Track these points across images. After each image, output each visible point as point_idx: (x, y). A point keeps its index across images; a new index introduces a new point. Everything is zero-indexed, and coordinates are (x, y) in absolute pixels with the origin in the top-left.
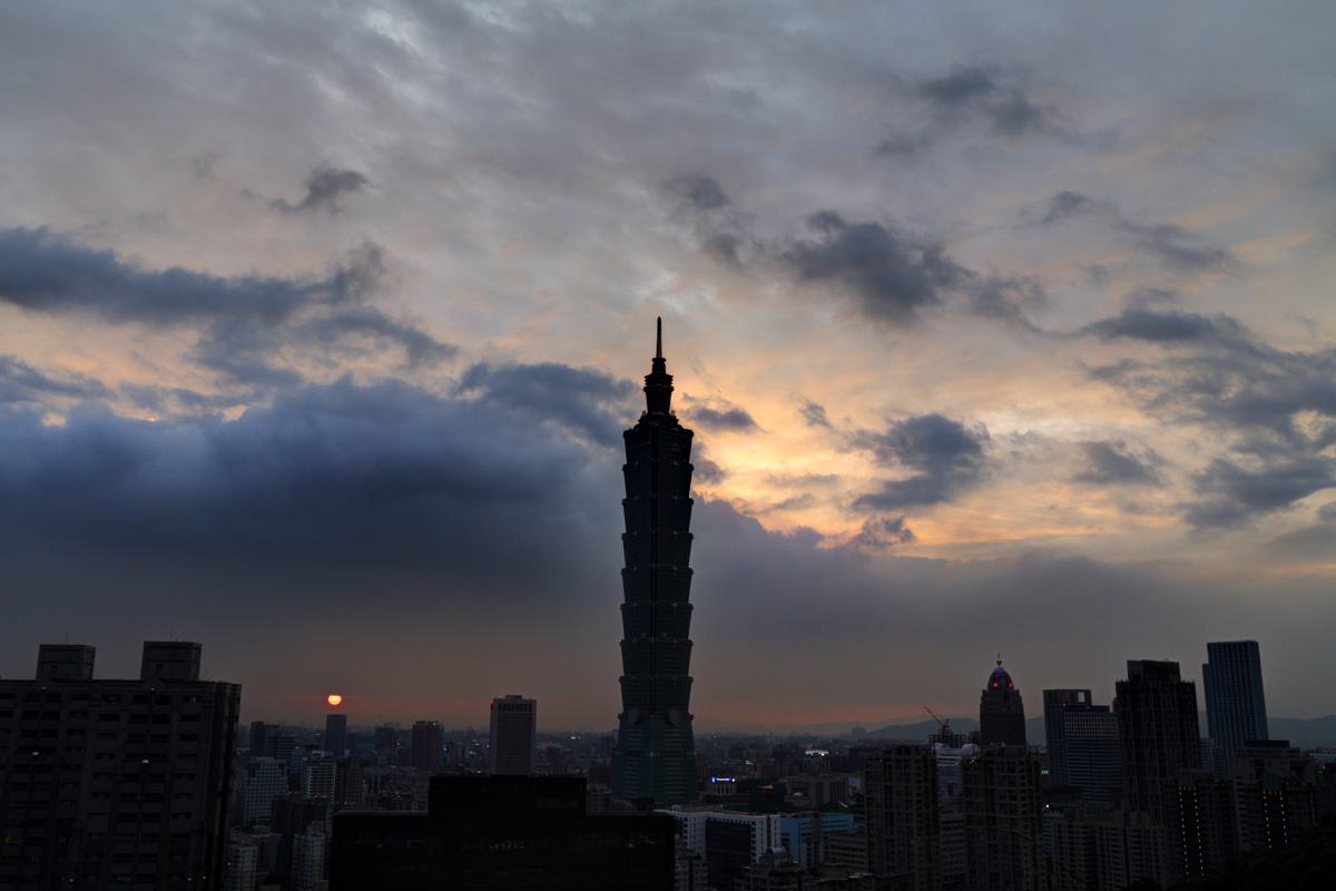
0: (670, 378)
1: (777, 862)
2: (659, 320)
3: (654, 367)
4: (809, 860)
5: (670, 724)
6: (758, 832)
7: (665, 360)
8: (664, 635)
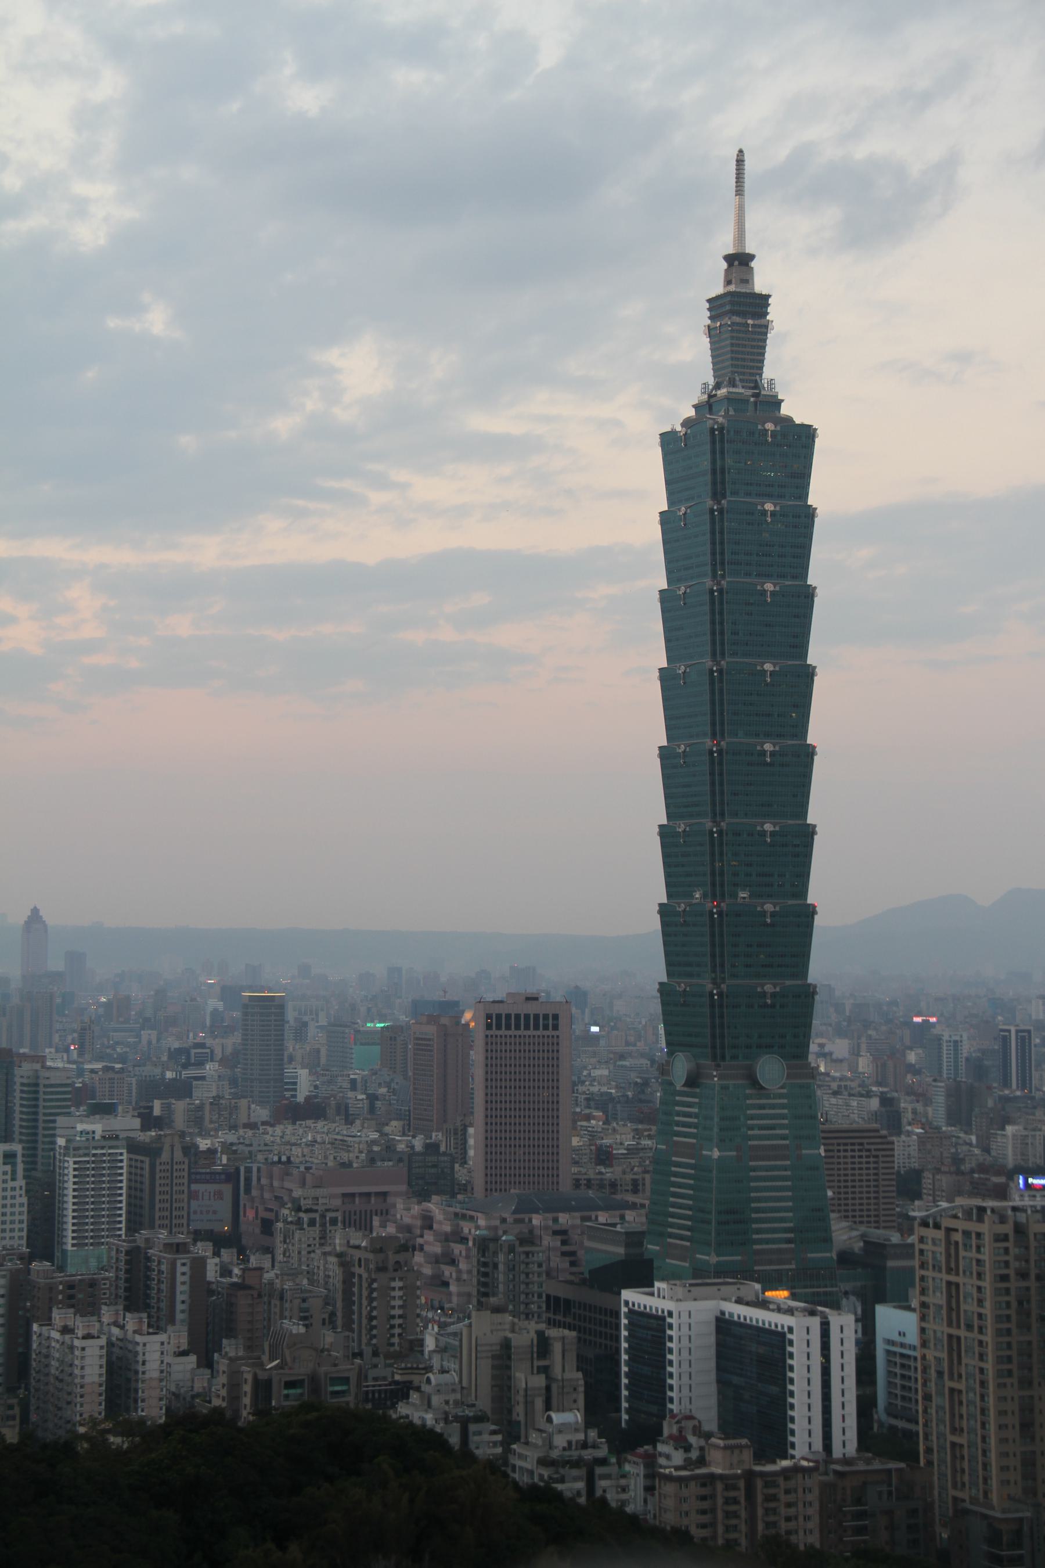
0: (763, 300)
1: (560, 1441)
2: (740, 162)
3: (728, 282)
5: (755, 1083)
6: (797, 1349)
7: (752, 257)
8: (742, 895)
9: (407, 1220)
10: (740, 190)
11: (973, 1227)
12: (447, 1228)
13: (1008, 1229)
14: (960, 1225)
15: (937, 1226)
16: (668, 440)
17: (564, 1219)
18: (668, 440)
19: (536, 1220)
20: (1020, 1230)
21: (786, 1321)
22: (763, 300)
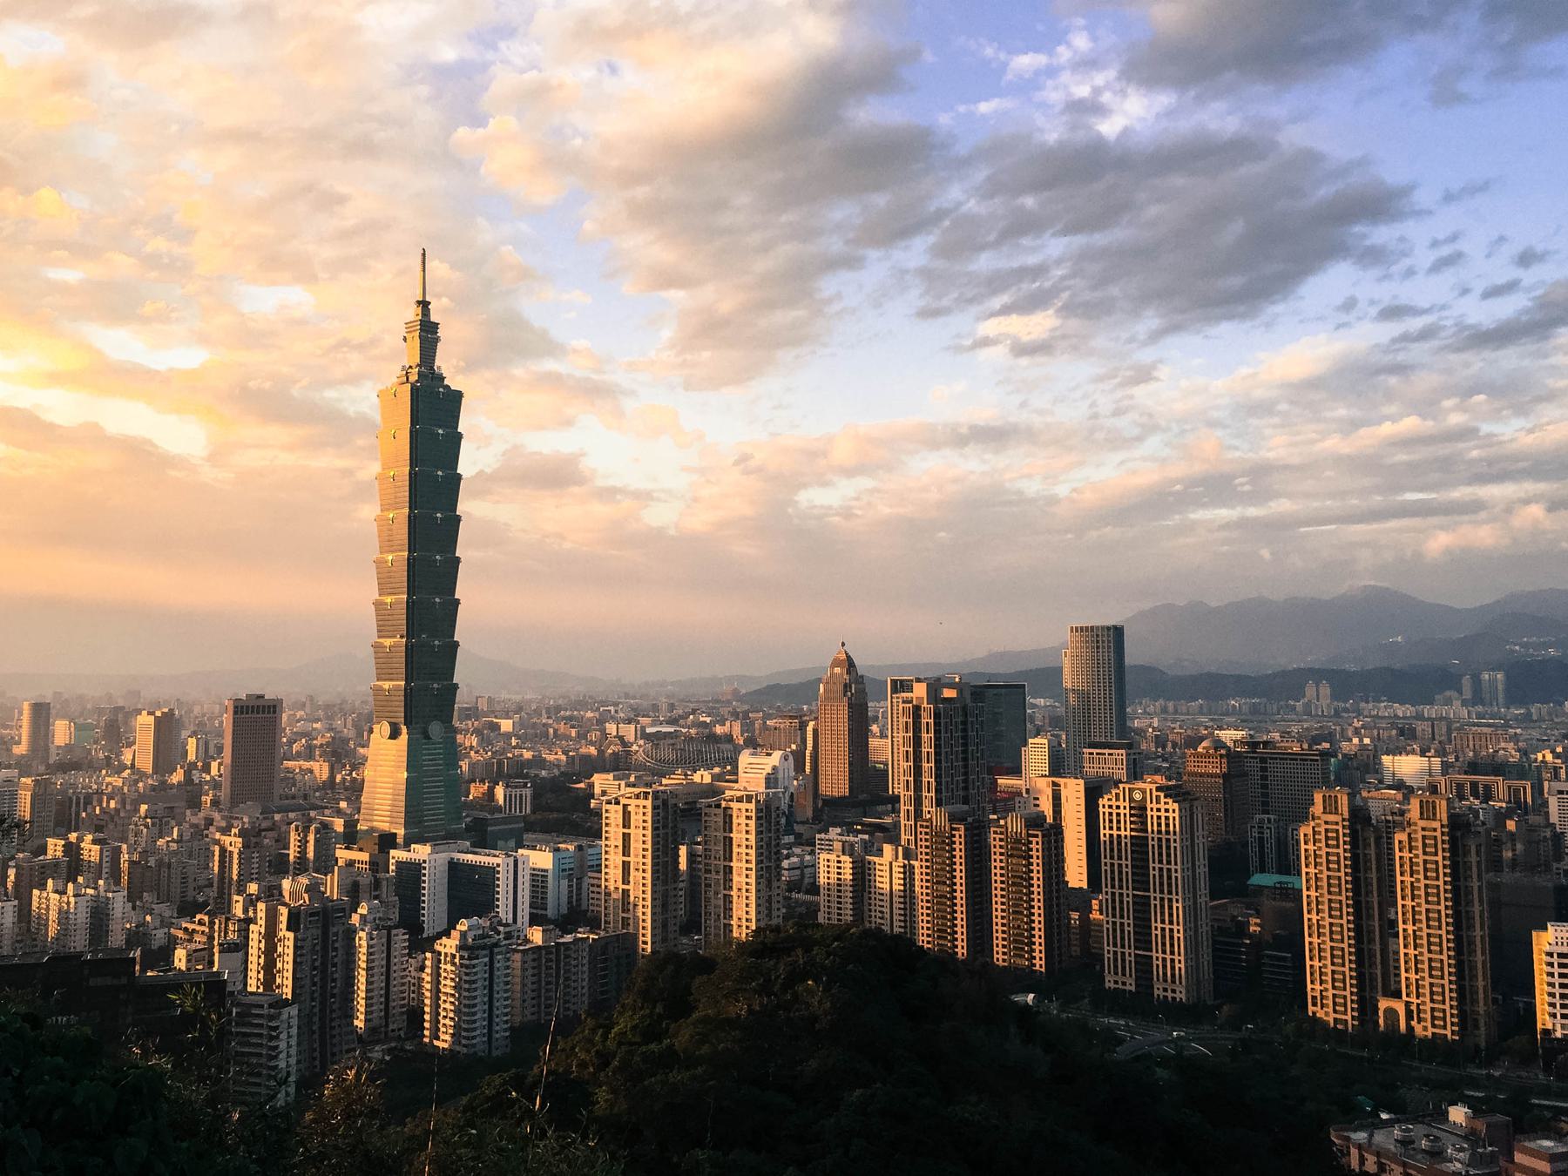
4: (570, 897)
5: (428, 737)
9: (194, 820)
11: (642, 802)
12: (223, 824)
13: (659, 802)
14: (633, 802)
15: (618, 803)
19: (277, 817)
20: (665, 803)
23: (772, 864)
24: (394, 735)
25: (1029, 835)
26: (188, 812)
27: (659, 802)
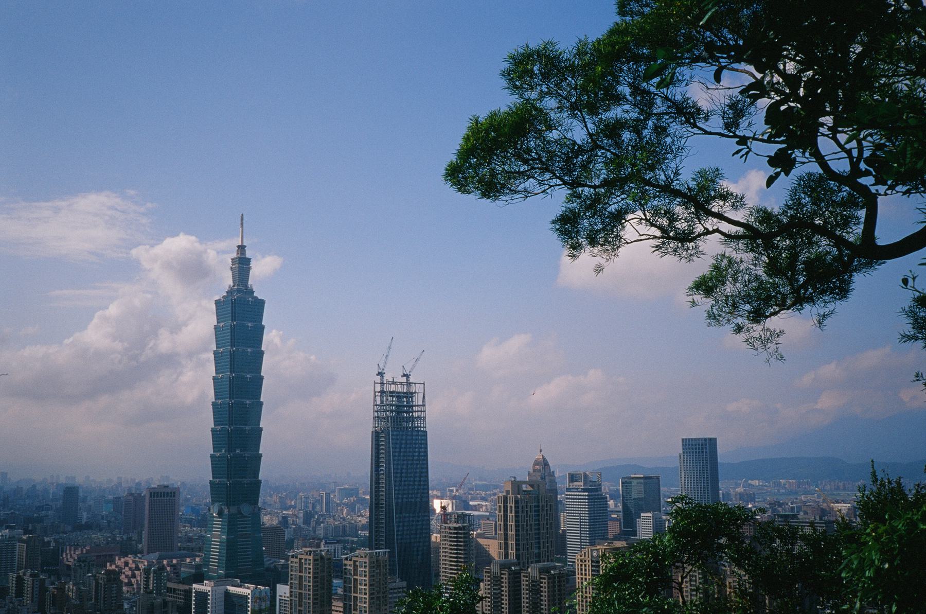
0: (249, 260)
2: (242, 217)
10: (242, 226)
11: (308, 557)
13: (318, 557)
16: (217, 303)
17: (175, 561)
18: (217, 303)
19: (165, 562)
21: (249, 591)
22: (249, 260)
23: (381, 595)
24: (220, 513)
25: (541, 578)
26: (117, 558)
27: (318, 557)
